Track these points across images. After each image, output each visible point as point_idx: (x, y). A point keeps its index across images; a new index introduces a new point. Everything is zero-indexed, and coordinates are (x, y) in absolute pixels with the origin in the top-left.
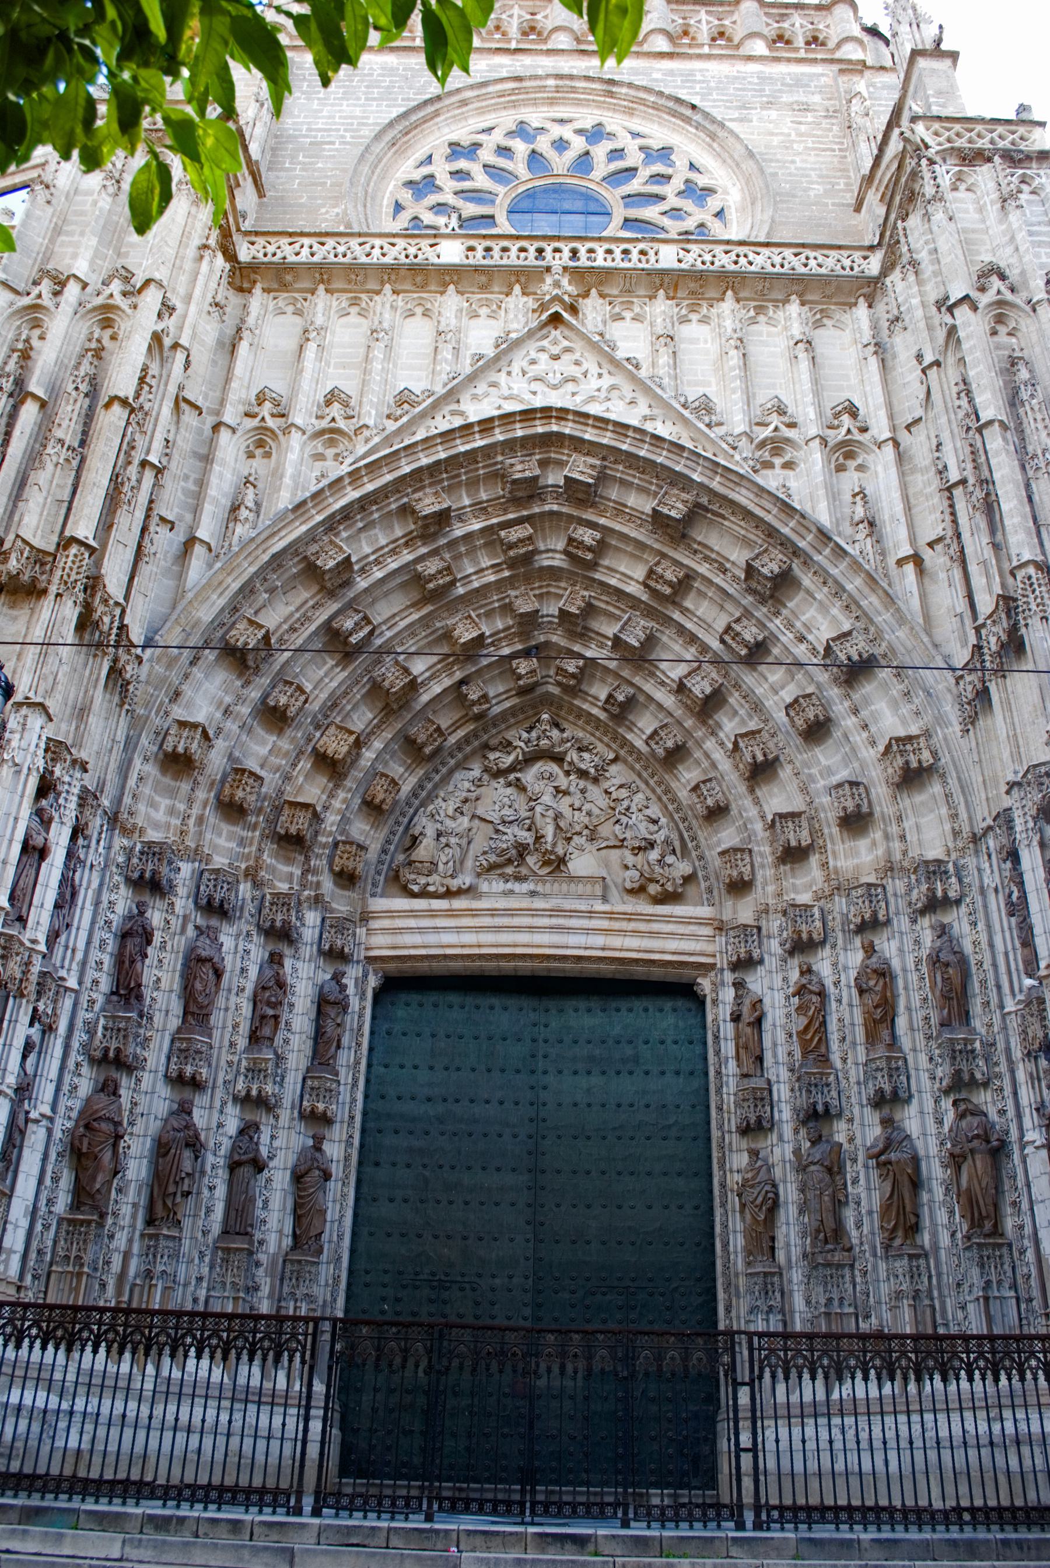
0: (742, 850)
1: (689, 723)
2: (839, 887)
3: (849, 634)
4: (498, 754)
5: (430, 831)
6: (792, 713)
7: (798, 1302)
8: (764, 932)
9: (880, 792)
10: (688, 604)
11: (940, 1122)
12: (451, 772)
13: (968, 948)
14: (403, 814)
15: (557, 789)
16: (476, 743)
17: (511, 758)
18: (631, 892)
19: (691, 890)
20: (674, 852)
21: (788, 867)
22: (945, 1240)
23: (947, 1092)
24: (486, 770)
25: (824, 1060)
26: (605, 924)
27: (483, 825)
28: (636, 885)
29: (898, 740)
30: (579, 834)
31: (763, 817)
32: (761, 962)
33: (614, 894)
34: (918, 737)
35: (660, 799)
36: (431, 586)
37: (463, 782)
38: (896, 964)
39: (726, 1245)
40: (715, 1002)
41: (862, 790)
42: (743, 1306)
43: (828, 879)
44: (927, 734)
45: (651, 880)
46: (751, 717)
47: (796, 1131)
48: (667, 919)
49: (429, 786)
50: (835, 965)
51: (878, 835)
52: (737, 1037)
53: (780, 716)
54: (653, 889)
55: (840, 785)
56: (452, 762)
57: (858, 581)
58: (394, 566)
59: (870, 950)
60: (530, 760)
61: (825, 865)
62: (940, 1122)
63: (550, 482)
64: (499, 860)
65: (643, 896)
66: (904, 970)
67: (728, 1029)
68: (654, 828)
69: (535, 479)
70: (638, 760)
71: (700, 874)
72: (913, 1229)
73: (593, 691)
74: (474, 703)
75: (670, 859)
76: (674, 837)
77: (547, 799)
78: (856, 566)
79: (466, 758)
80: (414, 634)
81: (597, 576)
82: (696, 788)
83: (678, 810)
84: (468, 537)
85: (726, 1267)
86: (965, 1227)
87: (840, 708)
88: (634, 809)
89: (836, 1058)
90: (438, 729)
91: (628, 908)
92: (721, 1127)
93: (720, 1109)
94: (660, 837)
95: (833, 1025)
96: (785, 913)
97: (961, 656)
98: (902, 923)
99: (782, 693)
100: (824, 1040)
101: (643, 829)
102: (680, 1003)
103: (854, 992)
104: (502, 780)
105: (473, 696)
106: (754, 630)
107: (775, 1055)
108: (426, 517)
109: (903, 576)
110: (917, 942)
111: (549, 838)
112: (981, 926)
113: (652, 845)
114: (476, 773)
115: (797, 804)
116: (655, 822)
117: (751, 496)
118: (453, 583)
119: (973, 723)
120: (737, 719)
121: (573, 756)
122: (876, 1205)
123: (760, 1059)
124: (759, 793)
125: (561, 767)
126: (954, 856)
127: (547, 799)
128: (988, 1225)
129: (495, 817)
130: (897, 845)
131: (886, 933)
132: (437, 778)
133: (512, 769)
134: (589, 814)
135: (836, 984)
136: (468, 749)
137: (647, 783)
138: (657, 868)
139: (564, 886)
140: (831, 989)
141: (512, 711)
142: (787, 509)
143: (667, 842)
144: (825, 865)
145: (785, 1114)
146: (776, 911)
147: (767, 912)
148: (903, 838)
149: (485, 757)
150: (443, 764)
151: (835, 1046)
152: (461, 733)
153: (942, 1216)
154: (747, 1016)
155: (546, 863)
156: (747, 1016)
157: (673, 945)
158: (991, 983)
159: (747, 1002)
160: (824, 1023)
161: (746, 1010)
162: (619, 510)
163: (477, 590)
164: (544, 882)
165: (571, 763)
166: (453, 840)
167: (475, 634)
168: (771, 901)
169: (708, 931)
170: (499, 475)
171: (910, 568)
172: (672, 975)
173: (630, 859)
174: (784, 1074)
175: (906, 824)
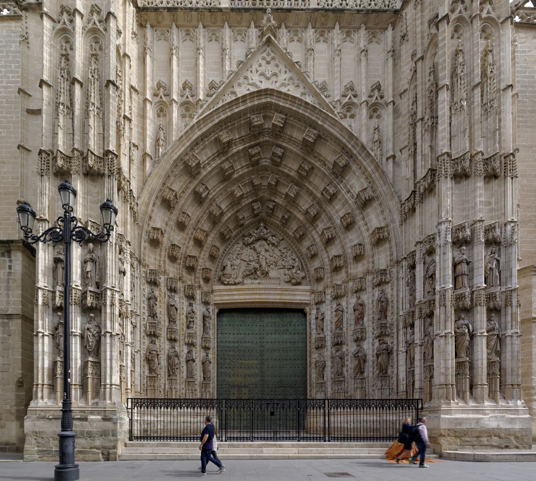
0: (321, 268)
2: (350, 278)
3: (366, 189)
4: (247, 238)
5: (229, 265)
7: (329, 390)
9: (368, 247)
10: (311, 180)
11: (373, 345)
13: (389, 296)
14: (221, 259)
16: (241, 235)
17: (252, 239)
18: (287, 282)
19: (304, 282)
22: (371, 375)
23: (376, 338)
24: (244, 244)
25: (342, 329)
26: (280, 292)
27: (244, 262)
29: (378, 228)
32: (324, 302)
33: (282, 283)
34: (384, 227)
35: (296, 252)
36: (227, 173)
37: (237, 248)
38: (366, 302)
39: (310, 376)
40: (310, 314)
41: (362, 247)
42: (314, 391)
43: (347, 277)
44: (387, 226)
45: (293, 279)
47: (332, 348)
49: (228, 250)
50: (347, 302)
51: (365, 262)
52: (316, 324)
53: (338, 222)
55: (355, 245)
56: (234, 241)
57: (373, 167)
58: (214, 165)
59: (359, 298)
60: (257, 240)
61: (347, 272)
62: (373, 345)
63: (266, 127)
65: (290, 283)
66: (369, 304)
67: (313, 321)
68: (294, 262)
69: (261, 125)
70: (290, 239)
71: (307, 276)
72: (362, 373)
74: (241, 220)
75: (298, 272)
77: (263, 253)
78: (373, 161)
79: (238, 240)
80: (221, 194)
81: (281, 169)
82: (308, 248)
84: (238, 152)
85: (310, 381)
86: (377, 372)
87: (359, 218)
89: (345, 329)
90: (230, 230)
91: (287, 287)
92: (310, 347)
93: (310, 343)
94: (296, 265)
95: (345, 320)
96: (334, 287)
97: (405, 195)
98: (369, 289)
100: (342, 324)
102: (300, 315)
103: (352, 310)
105: (241, 217)
106: (333, 188)
107: (327, 328)
108: (224, 143)
109: (387, 164)
110: (373, 295)
111: (264, 266)
112: (395, 290)
113: (293, 267)
114: (241, 245)
115: (340, 252)
116: (294, 260)
117: (339, 131)
118: (233, 173)
119: (405, 221)
121: (270, 238)
122: (353, 367)
123: (323, 329)
124: (328, 249)
126: (389, 268)
127: (263, 253)
128: (384, 372)
129: (247, 259)
130: (371, 265)
131: (364, 292)
132: (230, 247)
133: (252, 243)
135: (347, 308)
138: (295, 275)
140: (345, 309)
141: (252, 223)
142: (351, 136)
143: (298, 266)
144: (347, 272)
145: (329, 344)
148: (373, 262)
150: (231, 242)
151: (345, 325)
152: (236, 231)
153: (371, 369)
154: (320, 317)
155: (263, 274)
156: (320, 317)
157: (298, 298)
158: (395, 307)
159: (320, 314)
160: (342, 319)
161: (320, 316)
162: (291, 139)
163: (241, 176)
164: (262, 280)
166: (236, 267)
167: (241, 193)
170: (250, 124)
171: (391, 161)
172: (298, 307)
173: (287, 272)
174: (329, 333)
175: (375, 258)
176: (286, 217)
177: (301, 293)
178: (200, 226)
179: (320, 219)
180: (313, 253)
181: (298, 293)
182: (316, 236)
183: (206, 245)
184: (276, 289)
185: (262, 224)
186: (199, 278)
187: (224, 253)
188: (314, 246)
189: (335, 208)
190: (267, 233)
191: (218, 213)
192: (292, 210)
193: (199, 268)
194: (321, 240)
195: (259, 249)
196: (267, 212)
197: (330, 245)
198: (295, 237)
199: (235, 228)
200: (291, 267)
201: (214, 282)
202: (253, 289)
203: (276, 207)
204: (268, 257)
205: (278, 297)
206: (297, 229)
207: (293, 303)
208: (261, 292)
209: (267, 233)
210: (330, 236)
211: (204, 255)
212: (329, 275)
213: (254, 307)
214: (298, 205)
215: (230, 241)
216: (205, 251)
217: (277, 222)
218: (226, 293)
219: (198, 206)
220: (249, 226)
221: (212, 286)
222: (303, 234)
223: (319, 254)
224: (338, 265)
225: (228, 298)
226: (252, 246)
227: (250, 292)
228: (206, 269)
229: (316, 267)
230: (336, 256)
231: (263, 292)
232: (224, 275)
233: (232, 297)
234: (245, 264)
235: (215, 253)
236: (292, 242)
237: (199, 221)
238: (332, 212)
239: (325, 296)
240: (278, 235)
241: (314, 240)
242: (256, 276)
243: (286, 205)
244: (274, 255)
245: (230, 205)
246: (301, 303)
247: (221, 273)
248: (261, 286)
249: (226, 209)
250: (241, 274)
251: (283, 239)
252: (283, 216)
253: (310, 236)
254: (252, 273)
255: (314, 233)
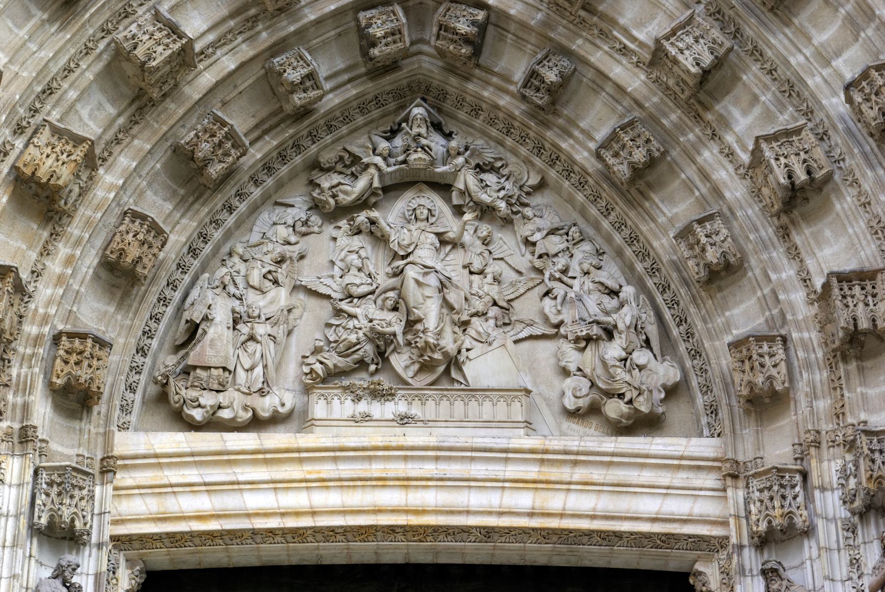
0: (771, 339)
1: (673, 117)
4: (336, 179)
5: (222, 312)
6: (858, 98)
8: (814, 479)
12: (255, 209)
15: (443, 240)
16: (298, 160)
17: (362, 183)
18: (574, 414)
19: (677, 413)
20: (647, 343)
21: (853, 366)
24: (316, 206)
26: (532, 472)
27: (313, 303)
28: (583, 403)
30: (483, 314)
31: (806, 281)
33: (548, 418)
35: (619, 253)
45: (609, 394)
46: (782, 108)
48: (641, 461)
49: (217, 235)
54: (614, 409)
56: (257, 193)
64: (341, 362)
65: (594, 421)
68: (610, 303)
70: (581, 185)
71: (694, 382)
73: (500, 66)
74: (294, 88)
75: (641, 357)
76: (648, 317)
77: (425, 255)
79: (280, 185)
82: (686, 233)
83: (653, 271)
88: (575, 270)
90: (231, 135)
91: (573, 444)
94: (624, 318)
99: (838, 63)
101: (593, 304)
104: (343, 223)
105: (293, 75)
111: (431, 322)
113: (609, 333)
114: (298, 212)
116: (613, 293)
120: (757, 111)
121: (468, 179)
125: (448, 200)
127: (425, 255)
129: (333, 288)
132: (231, 220)
133: (362, 204)
134: (497, 280)
136: (284, 170)
137: (597, 227)
138: (621, 374)
139: (459, 405)
143: (637, 328)
146: (833, 444)
147: (817, 444)
149: (314, 185)
150: (240, 195)
152: (271, 142)
155: (426, 367)
157: (649, 505)
164: (423, 400)
165: (465, 192)
166: (261, 330)
168: (826, 426)
169: (710, 480)
173: (572, 358)
176: (551, 76)
177: (664, 478)
178: (54, 116)
179: (738, 90)
180: (712, 255)
181: (647, 476)
182: (723, 174)
183: (84, 212)
184: (506, 454)
185: (418, 111)
186: (25, 388)
187: (193, 252)
188: (718, 224)
189: (809, 39)
190: (449, 155)
191: (161, 55)
192: (578, 45)
193: (30, 329)
194: (756, 193)
195: (400, 236)
196: (441, 54)
197: (809, 218)
198: (607, 175)
199: (262, 130)
200: (596, 330)
201: (125, 409)
202: (366, 454)
203: (491, 29)
204: (459, 276)
205: (524, 500)
206: (613, 137)
207: (618, 535)
208: (414, 469)
209: (449, 155)
210: (801, 176)
211: (69, 261)
212: (821, 376)
213: (369, 558)
214: (614, 22)
215: (230, 191)
216: (78, 242)
217: (504, 101)
218: (192, 475)
219: (51, 21)
220: (347, 119)
221: (107, 437)
222: (652, 162)
223: (753, 261)
224: (864, 324)
225: (203, 503)
226: (362, 217)
227: (346, 470)
228: (71, 336)
229: (738, 332)
230: (843, 278)
231: (429, 469)
232: (187, 371)
233: (230, 502)
234: (324, 310)
235: (133, 252)
236: (595, 199)
237: (49, 91)
238: (796, 60)
239: (809, 498)
240: (514, 165)
241: (717, 192)
242: (385, 381)
243: (547, 24)
244: (494, 268)
245: (232, 15)
246: (668, 539)
247: (171, 360)
248: (415, 436)
249: (211, 37)
250: (292, 370)
251: (541, 186)
252: (533, 74)
253: (691, 172)
254: (362, 364)
255: (709, 155)
